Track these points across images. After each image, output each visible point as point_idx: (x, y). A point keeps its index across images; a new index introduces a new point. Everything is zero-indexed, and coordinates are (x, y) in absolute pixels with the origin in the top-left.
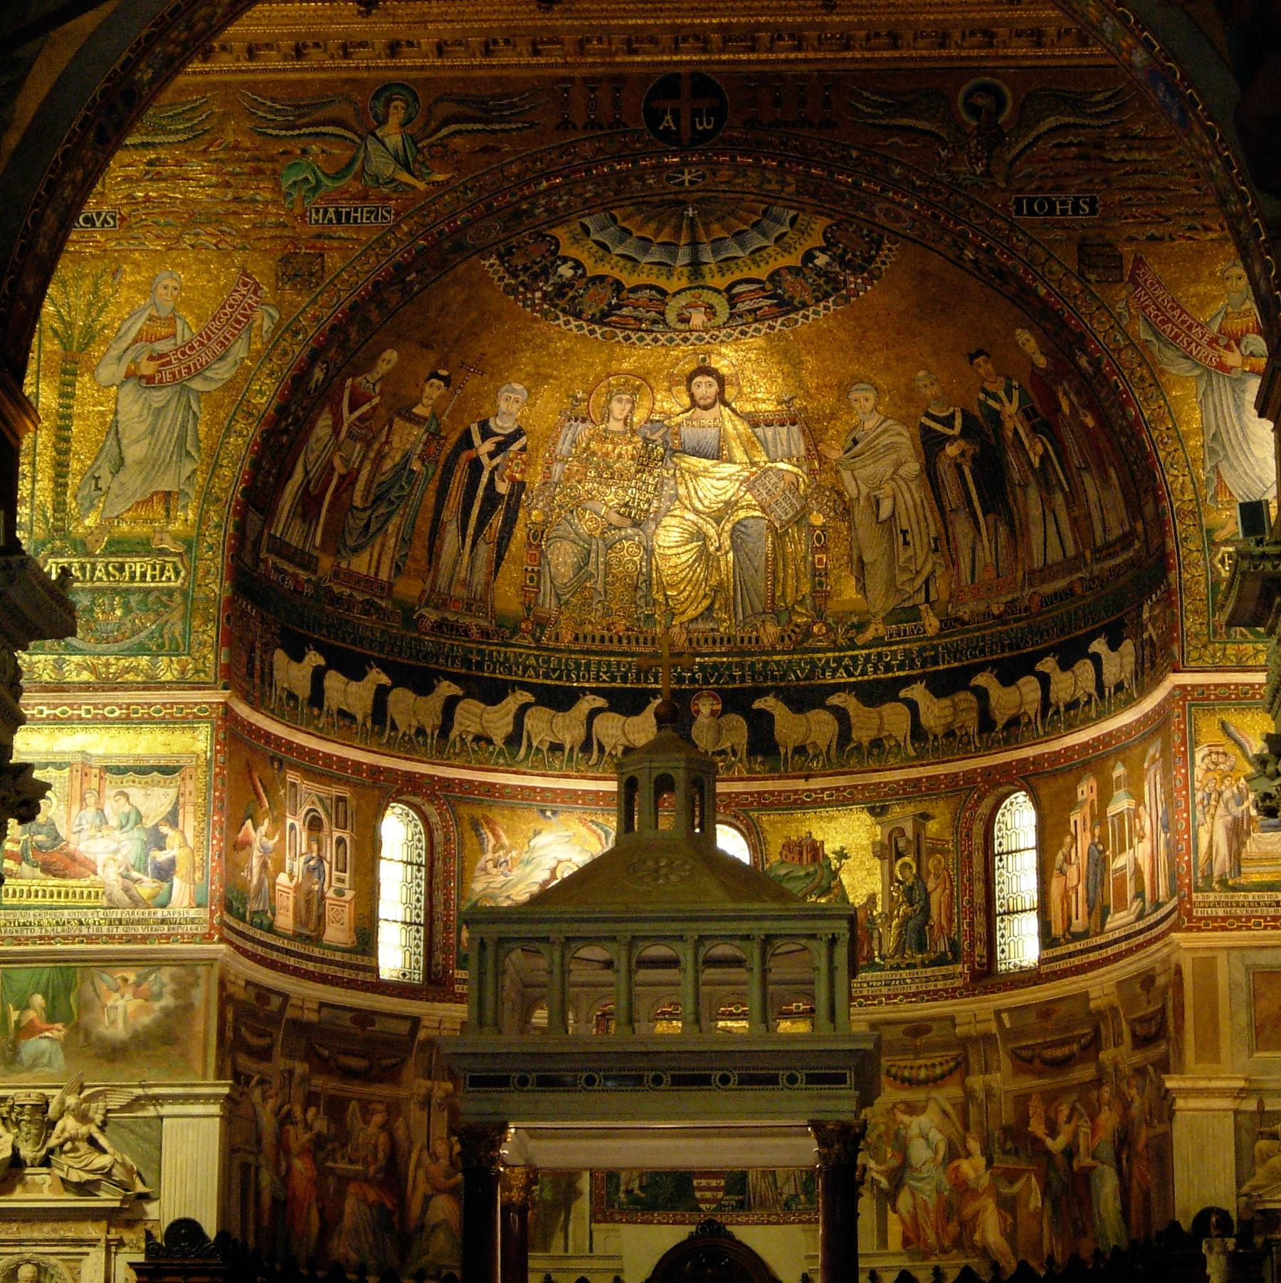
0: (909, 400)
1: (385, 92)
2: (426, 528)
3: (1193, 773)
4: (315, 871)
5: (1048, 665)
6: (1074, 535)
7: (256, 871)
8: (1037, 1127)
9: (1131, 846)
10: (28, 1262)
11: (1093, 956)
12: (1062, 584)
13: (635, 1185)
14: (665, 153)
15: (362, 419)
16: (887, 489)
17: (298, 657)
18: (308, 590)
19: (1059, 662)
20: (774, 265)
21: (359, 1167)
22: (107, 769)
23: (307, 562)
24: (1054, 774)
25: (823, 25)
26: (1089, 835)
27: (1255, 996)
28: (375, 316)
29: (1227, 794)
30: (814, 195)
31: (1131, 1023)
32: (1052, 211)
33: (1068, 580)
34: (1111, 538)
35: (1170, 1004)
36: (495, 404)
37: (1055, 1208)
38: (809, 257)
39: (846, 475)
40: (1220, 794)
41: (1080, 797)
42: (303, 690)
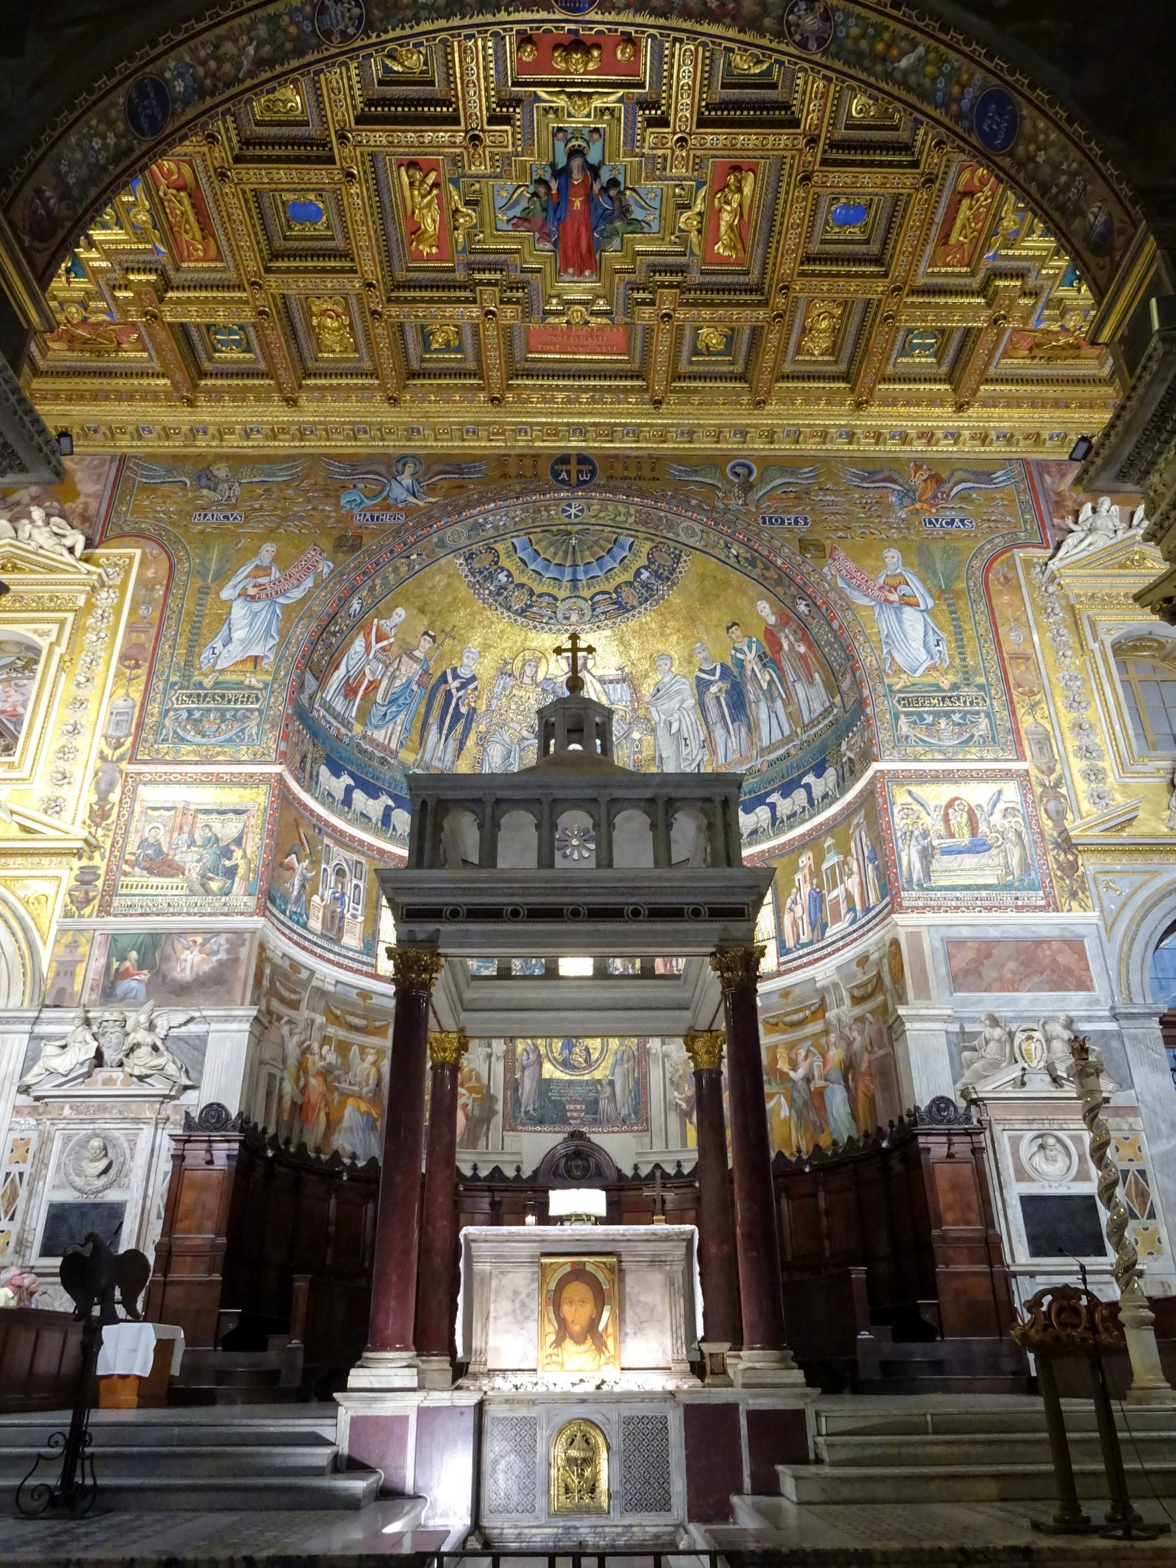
0: (690, 662)
1: (403, 459)
2: (419, 725)
4: (339, 899)
5: (775, 798)
7: (296, 887)
8: (783, 1065)
10: (97, 1136)
11: (816, 955)
13: (530, 1108)
14: (561, 490)
15: (384, 649)
16: (676, 716)
17: (338, 776)
18: (346, 740)
20: (618, 581)
21: (356, 1088)
22: (199, 811)
23: (346, 724)
24: (782, 856)
25: (651, 425)
27: (949, 957)
28: (391, 577)
29: (916, 833)
30: (645, 523)
31: (850, 991)
32: (783, 522)
34: (814, 716)
35: (886, 968)
36: (460, 659)
37: (800, 1116)
38: (638, 574)
39: (653, 710)
42: (340, 795)
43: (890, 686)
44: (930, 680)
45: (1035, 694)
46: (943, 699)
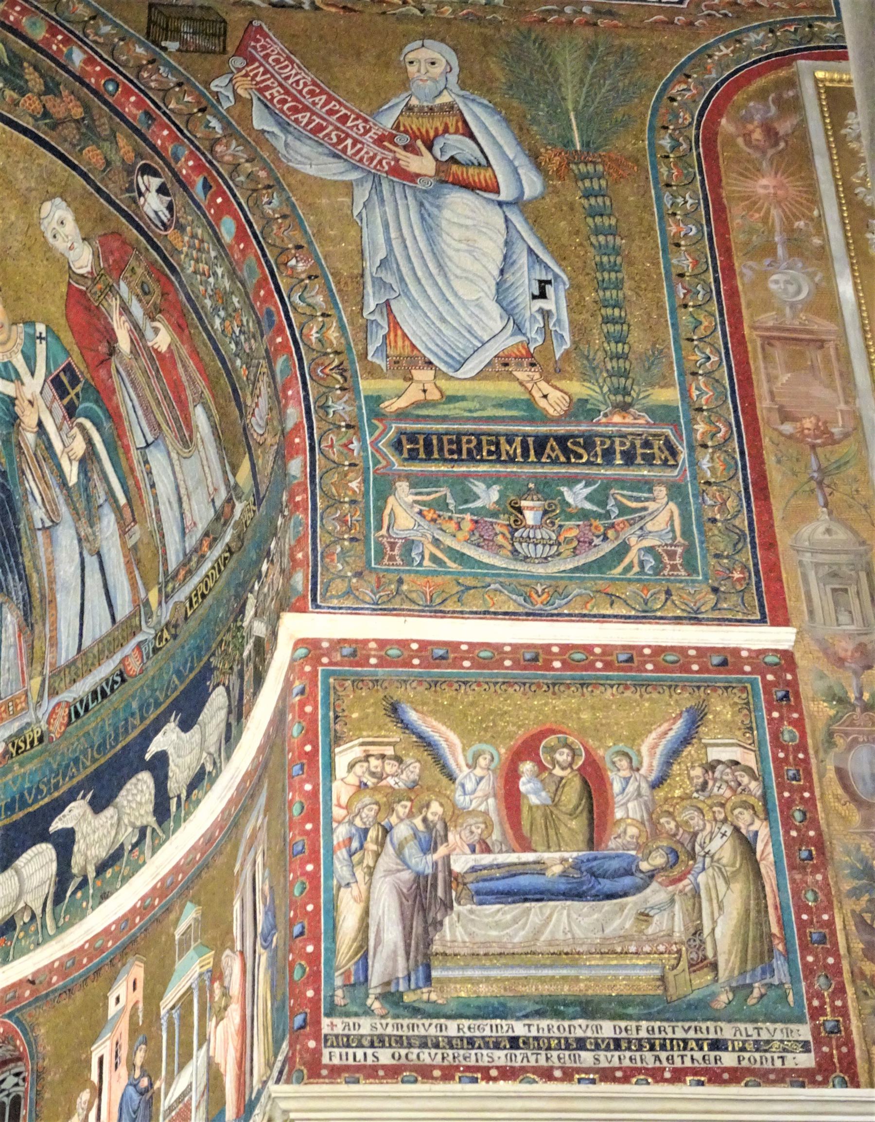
3: (329, 791)
6: (130, 573)
9: (204, 1039)
12: (106, 669)
19: (91, 803)
24: (68, 991)
26: (123, 1070)
29: (402, 831)
33: (118, 657)
34: (191, 542)
40: (387, 831)
41: (113, 1009)
43: (375, 401)
44: (507, 389)
45: (833, 441)
46: (541, 443)
